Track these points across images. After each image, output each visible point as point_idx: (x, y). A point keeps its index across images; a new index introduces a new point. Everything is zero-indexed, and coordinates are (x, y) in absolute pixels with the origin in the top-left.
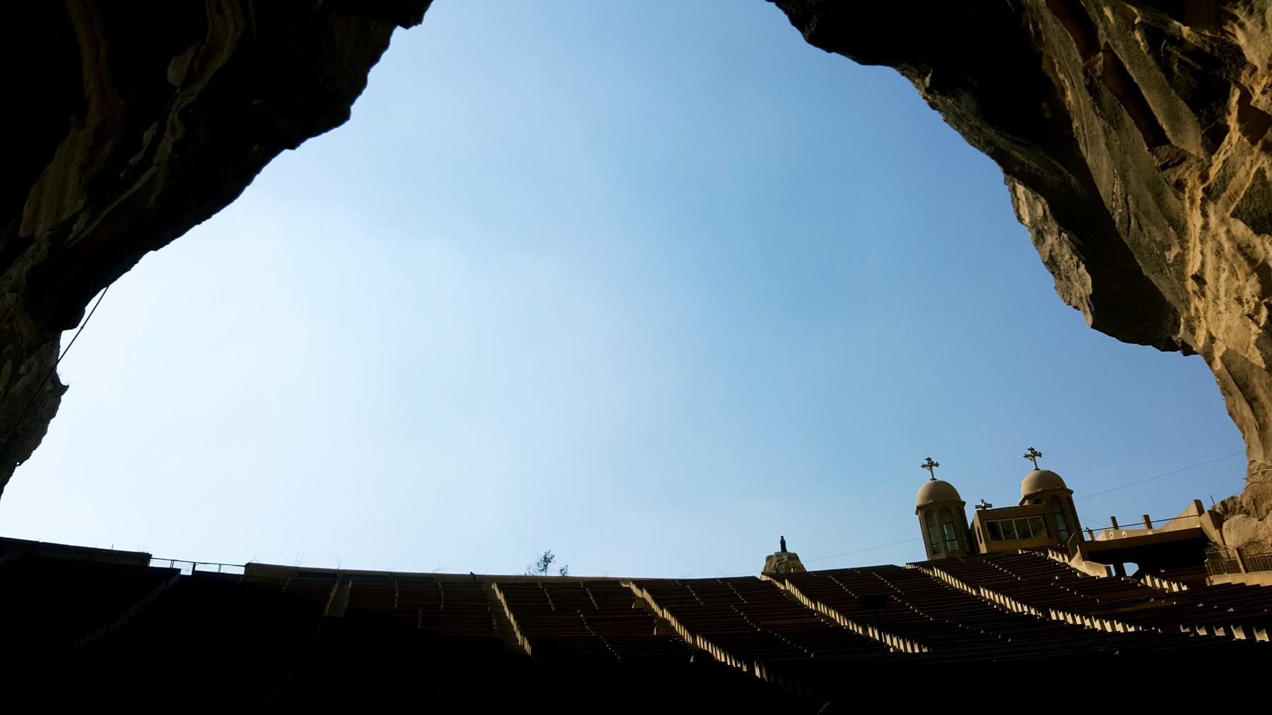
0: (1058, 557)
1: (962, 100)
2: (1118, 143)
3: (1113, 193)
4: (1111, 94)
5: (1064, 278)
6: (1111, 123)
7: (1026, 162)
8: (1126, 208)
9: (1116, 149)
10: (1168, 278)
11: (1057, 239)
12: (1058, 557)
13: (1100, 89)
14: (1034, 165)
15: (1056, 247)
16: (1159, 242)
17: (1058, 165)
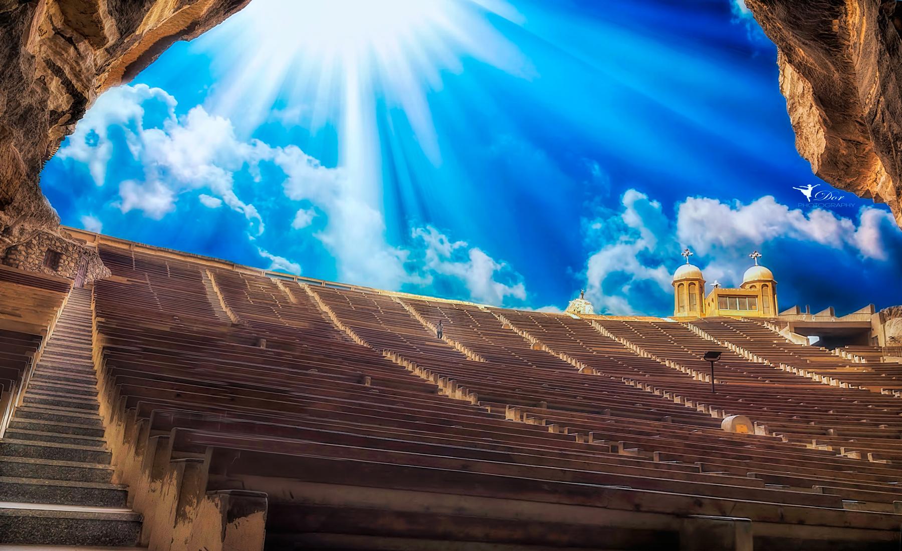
0: (771, 327)
1: (776, 9)
2: (888, 63)
3: (869, 94)
4: (896, 31)
5: (804, 138)
6: (888, 49)
7: (806, 57)
8: (876, 106)
9: (885, 67)
10: (893, 158)
11: (807, 111)
12: (771, 327)
13: (887, 25)
14: (811, 60)
15: (805, 116)
16: (895, 135)
17: (829, 64)
